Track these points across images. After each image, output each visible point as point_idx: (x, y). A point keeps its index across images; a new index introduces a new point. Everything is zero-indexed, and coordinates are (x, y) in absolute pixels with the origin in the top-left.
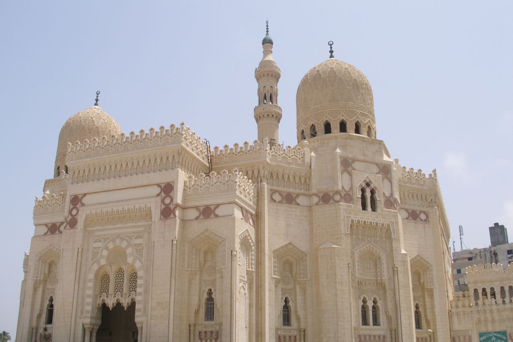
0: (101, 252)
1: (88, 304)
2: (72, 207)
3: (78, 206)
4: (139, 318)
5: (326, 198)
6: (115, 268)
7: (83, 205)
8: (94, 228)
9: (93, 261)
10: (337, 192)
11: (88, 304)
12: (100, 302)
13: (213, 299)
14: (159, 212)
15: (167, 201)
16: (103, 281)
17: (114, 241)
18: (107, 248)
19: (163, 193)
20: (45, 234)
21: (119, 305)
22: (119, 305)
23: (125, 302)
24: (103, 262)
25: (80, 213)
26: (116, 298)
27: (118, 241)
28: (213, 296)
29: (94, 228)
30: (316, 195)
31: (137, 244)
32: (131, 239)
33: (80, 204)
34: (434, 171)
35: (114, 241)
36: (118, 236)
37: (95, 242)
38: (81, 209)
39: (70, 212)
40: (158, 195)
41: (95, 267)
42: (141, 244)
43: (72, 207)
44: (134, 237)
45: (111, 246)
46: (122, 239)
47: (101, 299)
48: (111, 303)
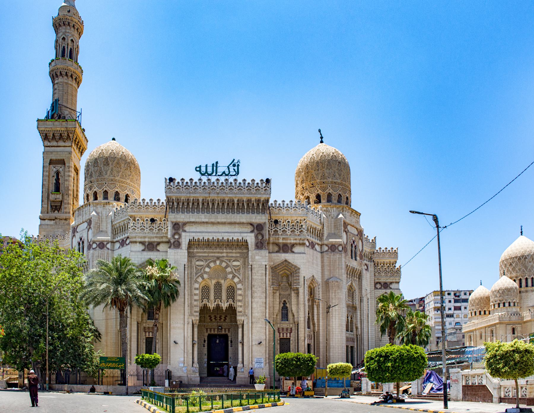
2: (174, 231)
4: (240, 318)
5: (333, 248)
6: (214, 282)
7: (185, 231)
10: (341, 245)
11: (196, 306)
12: (202, 305)
13: (287, 307)
14: (254, 244)
16: (205, 290)
17: (215, 262)
18: (208, 266)
19: (255, 231)
20: (143, 250)
21: (218, 307)
22: (218, 307)
23: (225, 305)
26: (216, 303)
27: (218, 262)
28: (288, 305)
30: (327, 245)
34: (375, 238)
35: (215, 262)
36: (218, 258)
38: (183, 234)
43: (174, 231)
46: (222, 261)
47: (203, 303)
48: (212, 305)
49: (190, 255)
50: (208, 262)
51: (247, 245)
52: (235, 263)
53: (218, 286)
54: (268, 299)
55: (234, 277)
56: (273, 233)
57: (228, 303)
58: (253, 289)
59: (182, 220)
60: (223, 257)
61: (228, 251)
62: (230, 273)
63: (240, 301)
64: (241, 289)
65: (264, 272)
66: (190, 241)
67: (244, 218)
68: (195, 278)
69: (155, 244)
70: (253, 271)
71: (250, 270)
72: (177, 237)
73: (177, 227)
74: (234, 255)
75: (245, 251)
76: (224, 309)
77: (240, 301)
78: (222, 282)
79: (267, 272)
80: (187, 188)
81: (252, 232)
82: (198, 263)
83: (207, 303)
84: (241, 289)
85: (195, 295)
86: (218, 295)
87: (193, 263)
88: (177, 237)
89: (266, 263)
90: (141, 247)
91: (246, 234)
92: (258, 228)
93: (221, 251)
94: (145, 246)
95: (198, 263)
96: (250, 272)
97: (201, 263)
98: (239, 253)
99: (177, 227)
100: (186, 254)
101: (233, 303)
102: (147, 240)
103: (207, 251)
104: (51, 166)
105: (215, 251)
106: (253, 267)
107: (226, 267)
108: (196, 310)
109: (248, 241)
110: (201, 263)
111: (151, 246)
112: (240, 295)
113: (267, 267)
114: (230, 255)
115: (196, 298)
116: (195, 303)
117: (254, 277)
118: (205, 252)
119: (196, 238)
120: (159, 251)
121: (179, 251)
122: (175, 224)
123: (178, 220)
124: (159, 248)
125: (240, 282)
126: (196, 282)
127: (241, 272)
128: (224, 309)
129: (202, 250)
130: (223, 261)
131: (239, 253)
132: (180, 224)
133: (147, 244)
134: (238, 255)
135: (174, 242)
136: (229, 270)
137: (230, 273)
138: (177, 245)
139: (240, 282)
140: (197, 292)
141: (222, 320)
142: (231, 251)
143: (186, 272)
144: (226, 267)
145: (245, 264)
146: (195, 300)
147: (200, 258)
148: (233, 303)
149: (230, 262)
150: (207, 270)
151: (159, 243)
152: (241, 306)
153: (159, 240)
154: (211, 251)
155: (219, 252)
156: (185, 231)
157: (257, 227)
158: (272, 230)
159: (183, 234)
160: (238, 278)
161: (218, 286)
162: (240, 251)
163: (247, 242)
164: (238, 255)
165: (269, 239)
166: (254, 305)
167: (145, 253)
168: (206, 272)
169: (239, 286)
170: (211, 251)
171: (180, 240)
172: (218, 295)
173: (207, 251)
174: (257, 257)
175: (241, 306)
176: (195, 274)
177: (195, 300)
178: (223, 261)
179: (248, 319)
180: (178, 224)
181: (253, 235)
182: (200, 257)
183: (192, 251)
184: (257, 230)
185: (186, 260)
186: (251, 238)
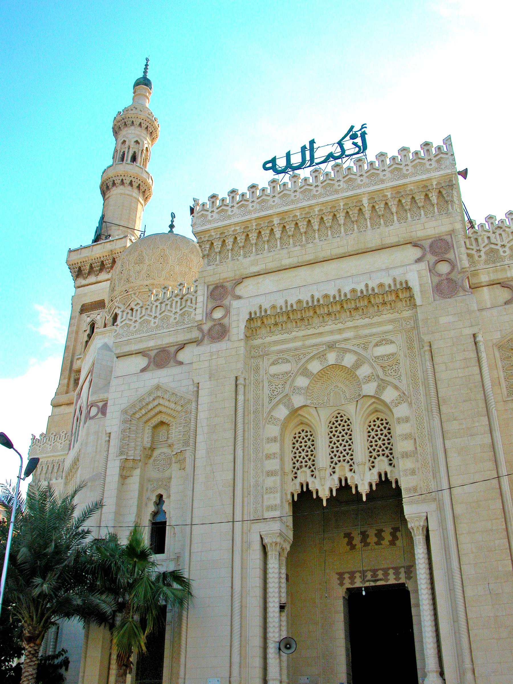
0: (293, 381)
1: (271, 490)
3: (226, 302)
7: (239, 297)
8: (268, 339)
9: (274, 402)
11: (271, 490)
15: (444, 268)
17: (321, 356)
18: (305, 372)
20: (143, 370)
21: (344, 488)
22: (344, 488)
23: (363, 481)
24: (298, 401)
25: (233, 312)
29: (268, 339)
31: (383, 356)
32: (365, 349)
33: (229, 297)
35: (321, 356)
36: (331, 346)
37: (273, 364)
39: (209, 315)
40: (419, 260)
41: (282, 412)
42: (393, 354)
43: (210, 306)
44: (374, 342)
45: (315, 367)
47: (298, 481)
49: (255, 355)
50: (304, 360)
51: (412, 297)
52: (380, 351)
53: (340, 426)
54: (497, 435)
55: (382, 385)
56: (483, 256)
57: (375, 471)
58: (444, 409)
59: (230, 275)
60: (346, 340)
61: (360, 322)
62: (368, 379)
63: (405, 455)
64: (407, 420)
65: (473, 355)
66: (251, 319)
67: (394, 231)
68: (266, 410)
69: (172, 350)
70: (436, 359)
71: (428, 356)
72: (218, 314)
73: (219, 293)
74: (375, 330)
75: (407, 314)
76: (364, 490)
77: (405, 455)
78: (350, 410)
79: (483, 355)
80: (243, 206)
81: (419, 260)
82: (274, 370)
83: (310, 480)
84: (407, 420)
85: (268, 457)
86: (342, 452)
87: (262, 372)
88: (218, 314)
89: (474, 330)
90: (141, 362)
91: (401, 270)
92: (439, 248)
93: (340, 326)
94: (150, 359)
95: (274, 370)
96: (429, 364)
97: (285, 367)
98: (391, 321)
99: (219, 293)
100: (242, 351)
101: (388, 469)
102: (151, 344)
103: (301, 333)
104: (84, 315)
105: (321, 330)
106: (433, 347)
107: (357, 365)
108: (272, 502)
109: (410, 284)
110: (285, 367)
111: (162, 358)
112: (406, 437)
113: (479, 338)
114: (366, 332)
115: (273, 465)
116: (270, 482)
117: (443, 375)
118: (295, 338)
119: (266, 305)
120: (181, 363)
121: (222, 345)
122: (216, 288)
123: (223, 276)
124: (182, 356)
125: (403, 398)
126: (271, 419)
127: (402, 371)
128: (364, 490)
129: (286, 336)
130: (346, 351)
131: (391, 321)
132: (228, 285)
133: (153, 354)
134: (390, 327)
135: (210, 330)
136: (364, 371)
137: (368, 379)
138: (219, 332)
139: (403, 398)
140: (274, 448)
141: (386, 542)
142: (367, 321)
143: (241, 398)
144: (357, 365)
145: (410, 348)
146: (271, 473)
147: (281, 355)
148: (388, 469)
149: (365, 349)
150: (302, 382)
151: (182, 347)
152: (413, 472)
153: (181, 338)
154: (311, 331)
155: (332, 332)
156: (239, 297)
157: (431, 246)
158: (479, 251)
159: (235, 304)
160: (396, 388)
161: (340, 426)
162: (396, 315)
163: (408, 288)
164: (390, 327)
165: (475, 274)
166: (454, 460)
167: (147, 375)
168: (297, 390)
169: (401, 411)
170: (311, 331)
171: (226, 321)
172: (342, 452)
173: (301, 333)
174: (443, 320)
175: (413, 472)
176: (266, 401)
177: (271, 473)
178: (346, 351)
179: (440, 508)
180: (222, 287)
181: (423, 266)
182: (282, 351)
183: (257, 342)
184: (434, 253)
185: (240, 365)
186: (418, 278)
